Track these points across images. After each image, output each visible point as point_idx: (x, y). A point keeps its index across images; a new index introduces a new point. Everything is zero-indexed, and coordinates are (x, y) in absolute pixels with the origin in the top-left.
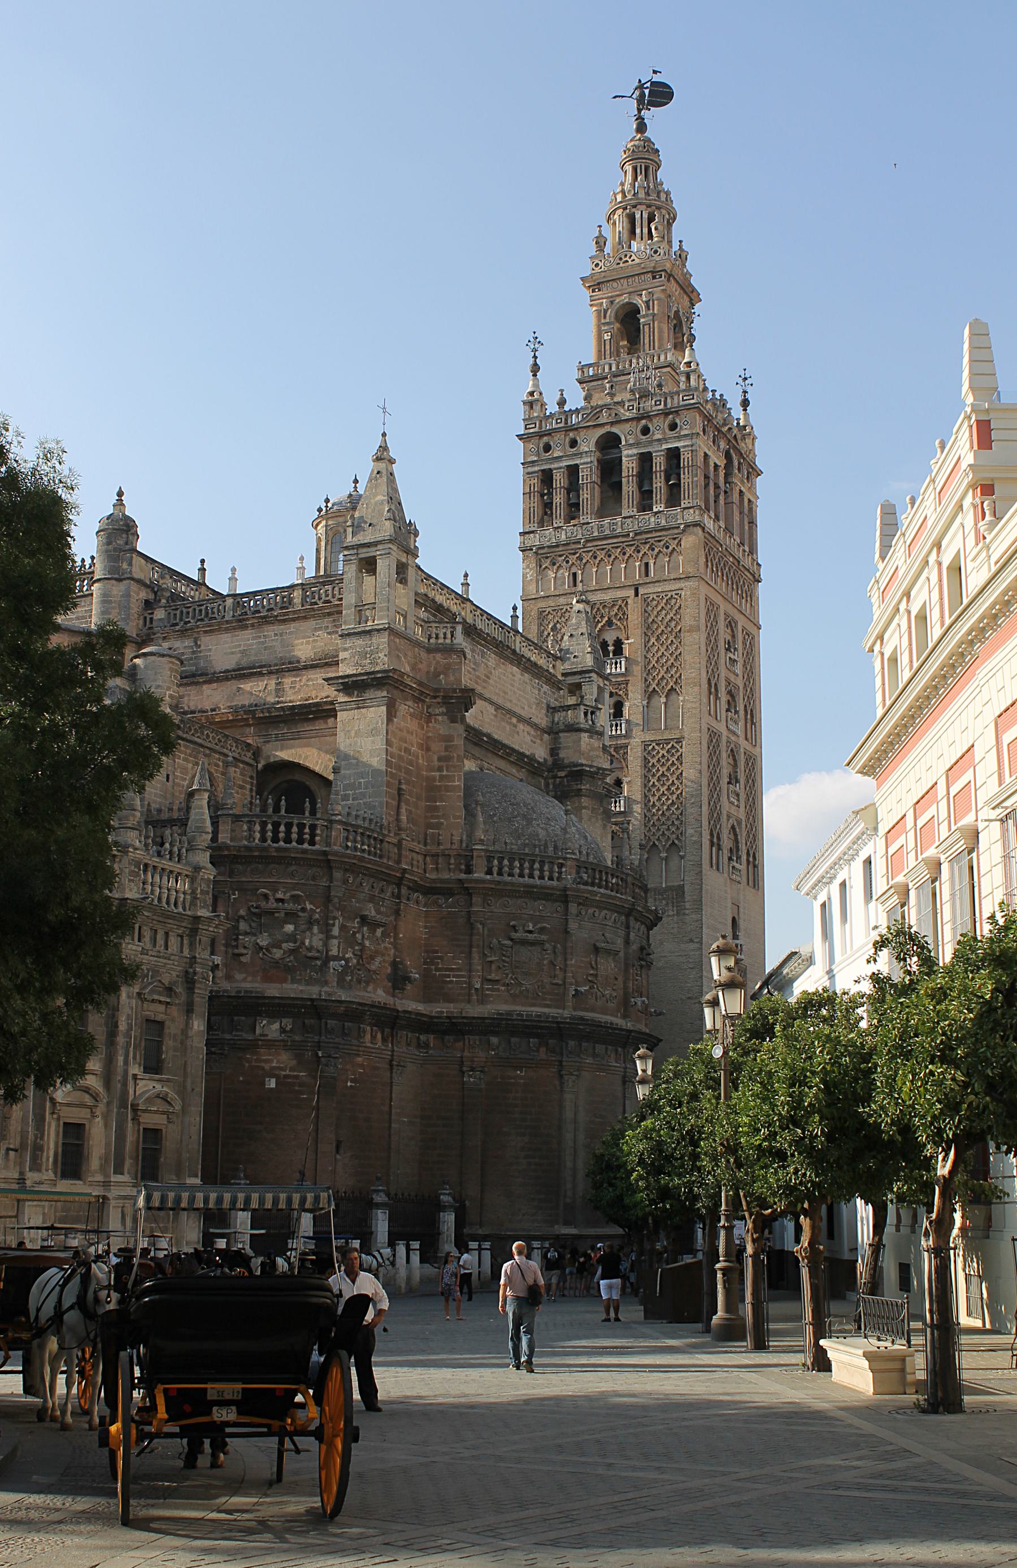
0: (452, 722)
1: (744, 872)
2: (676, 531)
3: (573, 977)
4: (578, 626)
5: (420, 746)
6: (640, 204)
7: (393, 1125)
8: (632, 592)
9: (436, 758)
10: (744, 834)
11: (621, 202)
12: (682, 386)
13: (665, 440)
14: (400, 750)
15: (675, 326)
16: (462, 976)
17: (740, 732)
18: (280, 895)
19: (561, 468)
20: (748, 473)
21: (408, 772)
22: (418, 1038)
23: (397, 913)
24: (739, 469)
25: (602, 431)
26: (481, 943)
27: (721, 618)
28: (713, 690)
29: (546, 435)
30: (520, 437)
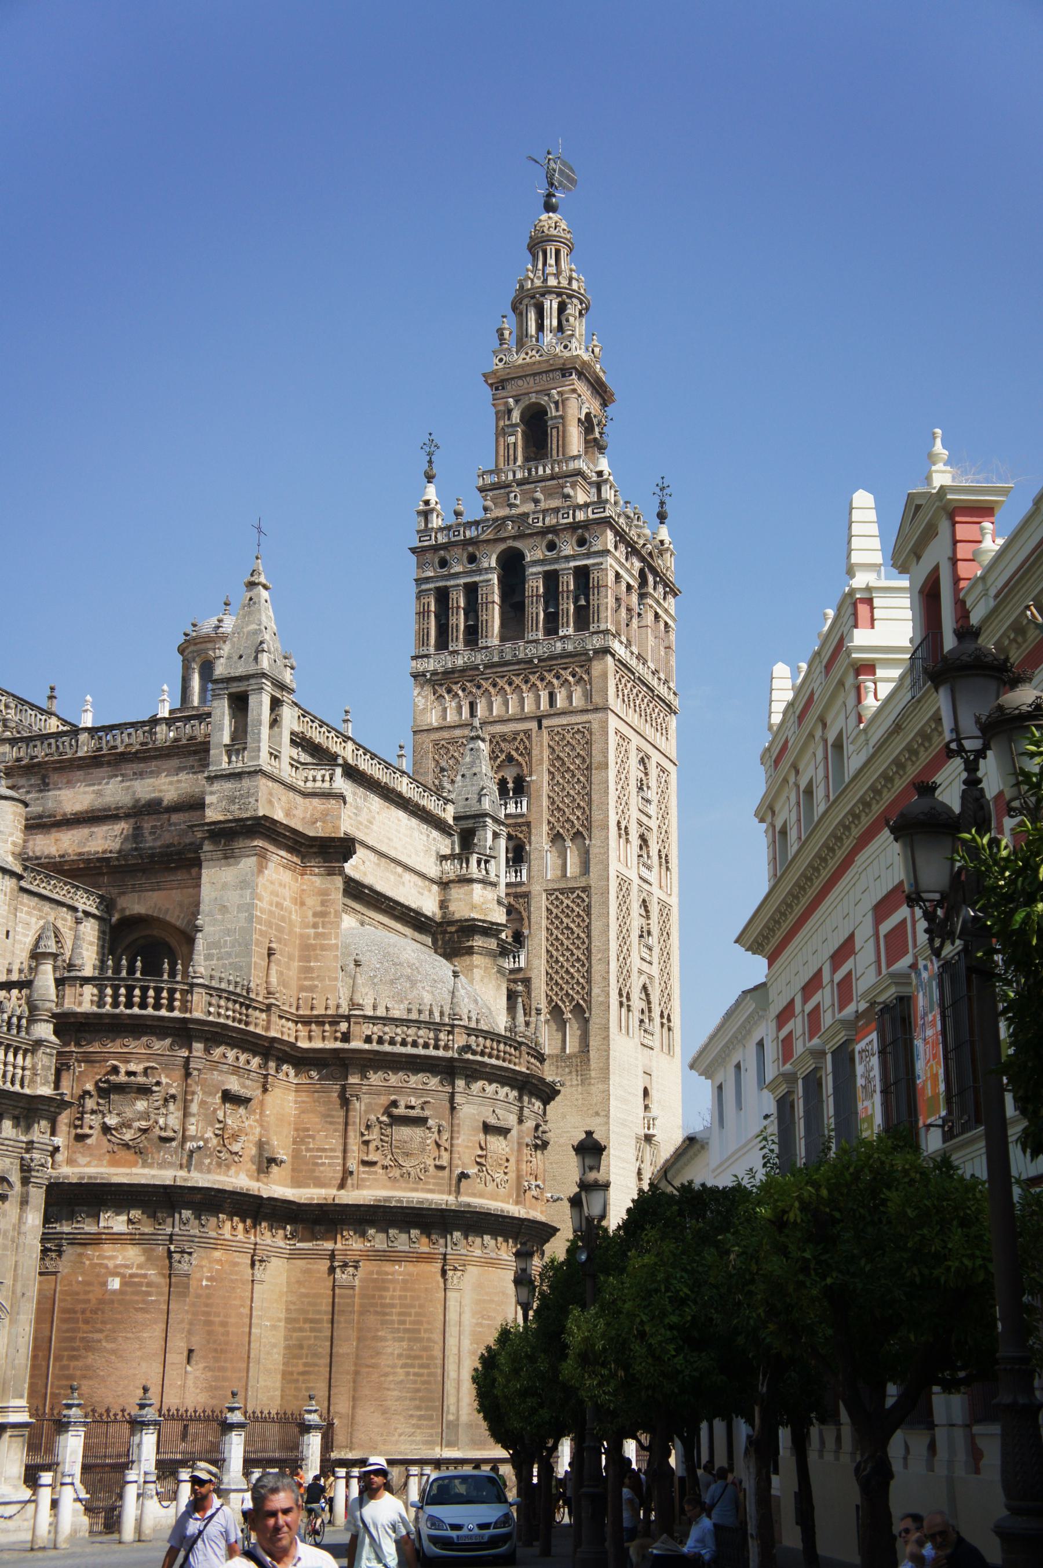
1: (657, 1035)
2: (583, 658)
5: (294, 901)
6: (550, 292)
7: (253, 1330)
8: (534, 725)
9: (310, 913)
10: (658, 992)
13: (574, 557)
14: (271, 905)
16: (337, 1157)
18: (133, 1067)
19: (458, 586)
21: (280, 930)
24: (655, 589)
25: (502, 547)
26: (358, 1120)
29: (441, 549)
30: (413, 550)
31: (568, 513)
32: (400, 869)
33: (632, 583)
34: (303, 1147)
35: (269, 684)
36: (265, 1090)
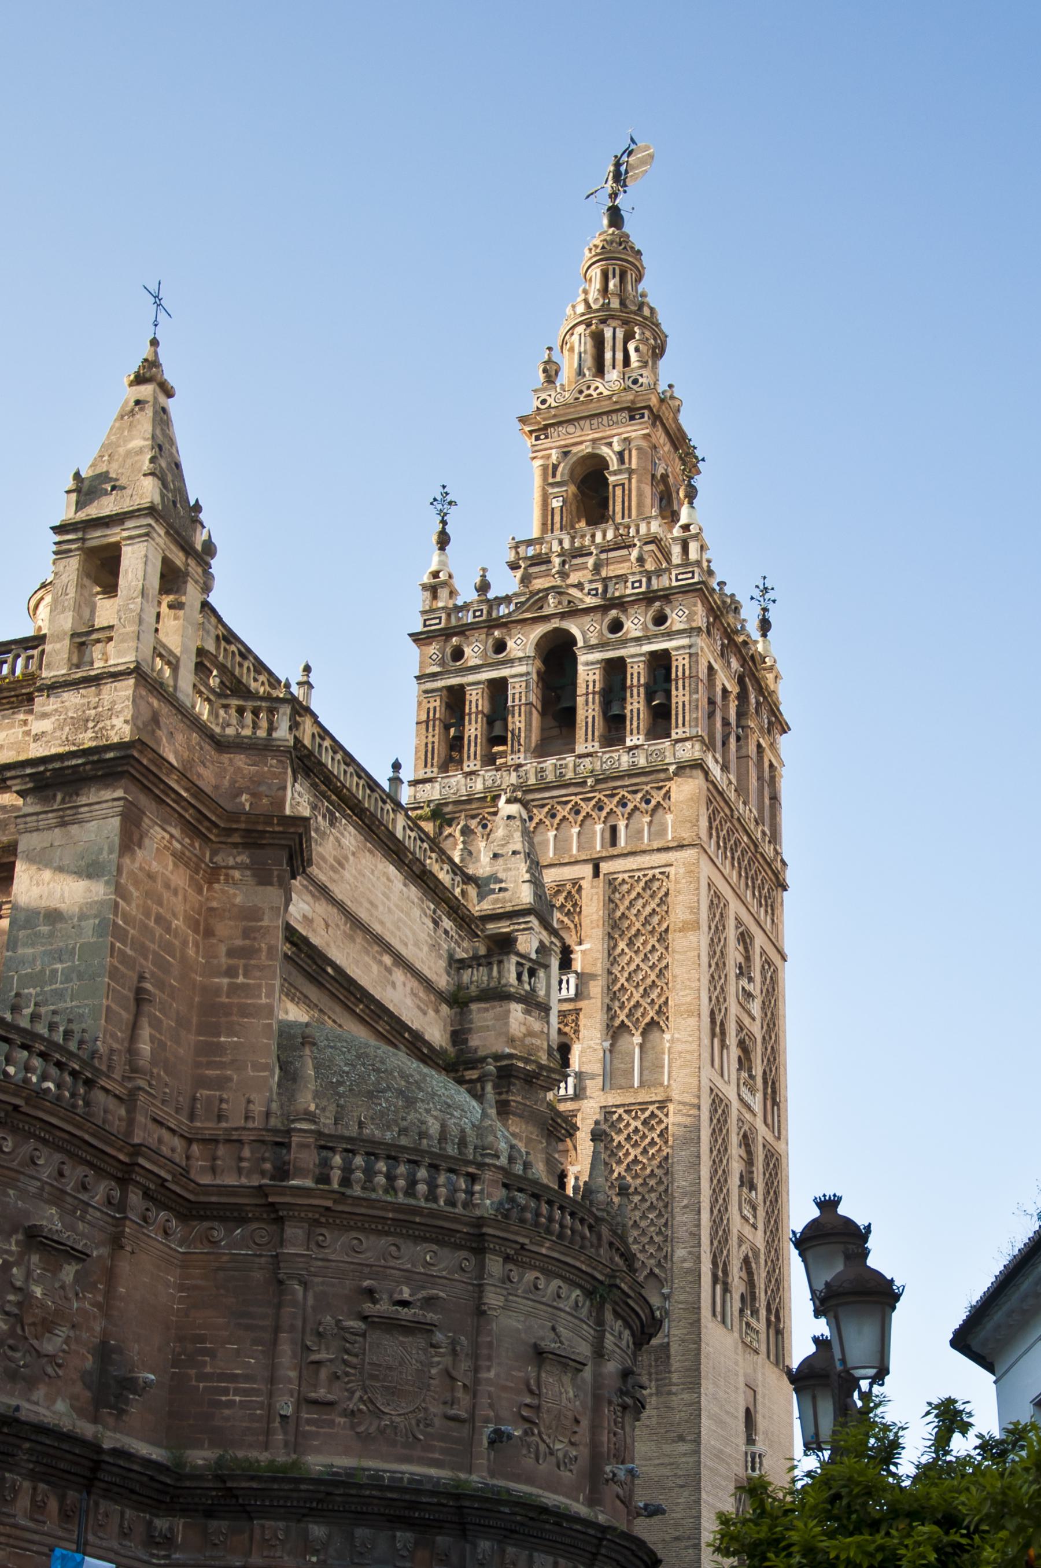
0: (261, 883)
1: (763, 1336)
2: (662, 776)
3: (491, 1406)
4: (507, 839)
5: (195, 926)
8: (588, 870)
9: (223, 949)
10: (763, 1274)
11: (583, 314)
12: (676, 559)
13: (647, 638)
15: (661, 493)
16: (256, 1392)
17: (758, 1107)
20: (770, 723)
22: (150, 1523)
23: (116, 1242)
26: (299, 1323)
27: (731, 923)
28: (718, 1030)
31: (640, 581)
32: (387, 960)
33: (729, 688)
34: (192, 1372)
35: (162, 532)
36: (116, 1242)
